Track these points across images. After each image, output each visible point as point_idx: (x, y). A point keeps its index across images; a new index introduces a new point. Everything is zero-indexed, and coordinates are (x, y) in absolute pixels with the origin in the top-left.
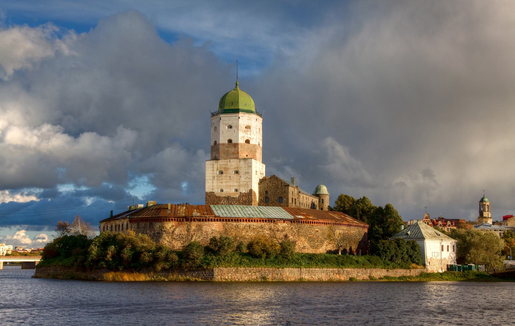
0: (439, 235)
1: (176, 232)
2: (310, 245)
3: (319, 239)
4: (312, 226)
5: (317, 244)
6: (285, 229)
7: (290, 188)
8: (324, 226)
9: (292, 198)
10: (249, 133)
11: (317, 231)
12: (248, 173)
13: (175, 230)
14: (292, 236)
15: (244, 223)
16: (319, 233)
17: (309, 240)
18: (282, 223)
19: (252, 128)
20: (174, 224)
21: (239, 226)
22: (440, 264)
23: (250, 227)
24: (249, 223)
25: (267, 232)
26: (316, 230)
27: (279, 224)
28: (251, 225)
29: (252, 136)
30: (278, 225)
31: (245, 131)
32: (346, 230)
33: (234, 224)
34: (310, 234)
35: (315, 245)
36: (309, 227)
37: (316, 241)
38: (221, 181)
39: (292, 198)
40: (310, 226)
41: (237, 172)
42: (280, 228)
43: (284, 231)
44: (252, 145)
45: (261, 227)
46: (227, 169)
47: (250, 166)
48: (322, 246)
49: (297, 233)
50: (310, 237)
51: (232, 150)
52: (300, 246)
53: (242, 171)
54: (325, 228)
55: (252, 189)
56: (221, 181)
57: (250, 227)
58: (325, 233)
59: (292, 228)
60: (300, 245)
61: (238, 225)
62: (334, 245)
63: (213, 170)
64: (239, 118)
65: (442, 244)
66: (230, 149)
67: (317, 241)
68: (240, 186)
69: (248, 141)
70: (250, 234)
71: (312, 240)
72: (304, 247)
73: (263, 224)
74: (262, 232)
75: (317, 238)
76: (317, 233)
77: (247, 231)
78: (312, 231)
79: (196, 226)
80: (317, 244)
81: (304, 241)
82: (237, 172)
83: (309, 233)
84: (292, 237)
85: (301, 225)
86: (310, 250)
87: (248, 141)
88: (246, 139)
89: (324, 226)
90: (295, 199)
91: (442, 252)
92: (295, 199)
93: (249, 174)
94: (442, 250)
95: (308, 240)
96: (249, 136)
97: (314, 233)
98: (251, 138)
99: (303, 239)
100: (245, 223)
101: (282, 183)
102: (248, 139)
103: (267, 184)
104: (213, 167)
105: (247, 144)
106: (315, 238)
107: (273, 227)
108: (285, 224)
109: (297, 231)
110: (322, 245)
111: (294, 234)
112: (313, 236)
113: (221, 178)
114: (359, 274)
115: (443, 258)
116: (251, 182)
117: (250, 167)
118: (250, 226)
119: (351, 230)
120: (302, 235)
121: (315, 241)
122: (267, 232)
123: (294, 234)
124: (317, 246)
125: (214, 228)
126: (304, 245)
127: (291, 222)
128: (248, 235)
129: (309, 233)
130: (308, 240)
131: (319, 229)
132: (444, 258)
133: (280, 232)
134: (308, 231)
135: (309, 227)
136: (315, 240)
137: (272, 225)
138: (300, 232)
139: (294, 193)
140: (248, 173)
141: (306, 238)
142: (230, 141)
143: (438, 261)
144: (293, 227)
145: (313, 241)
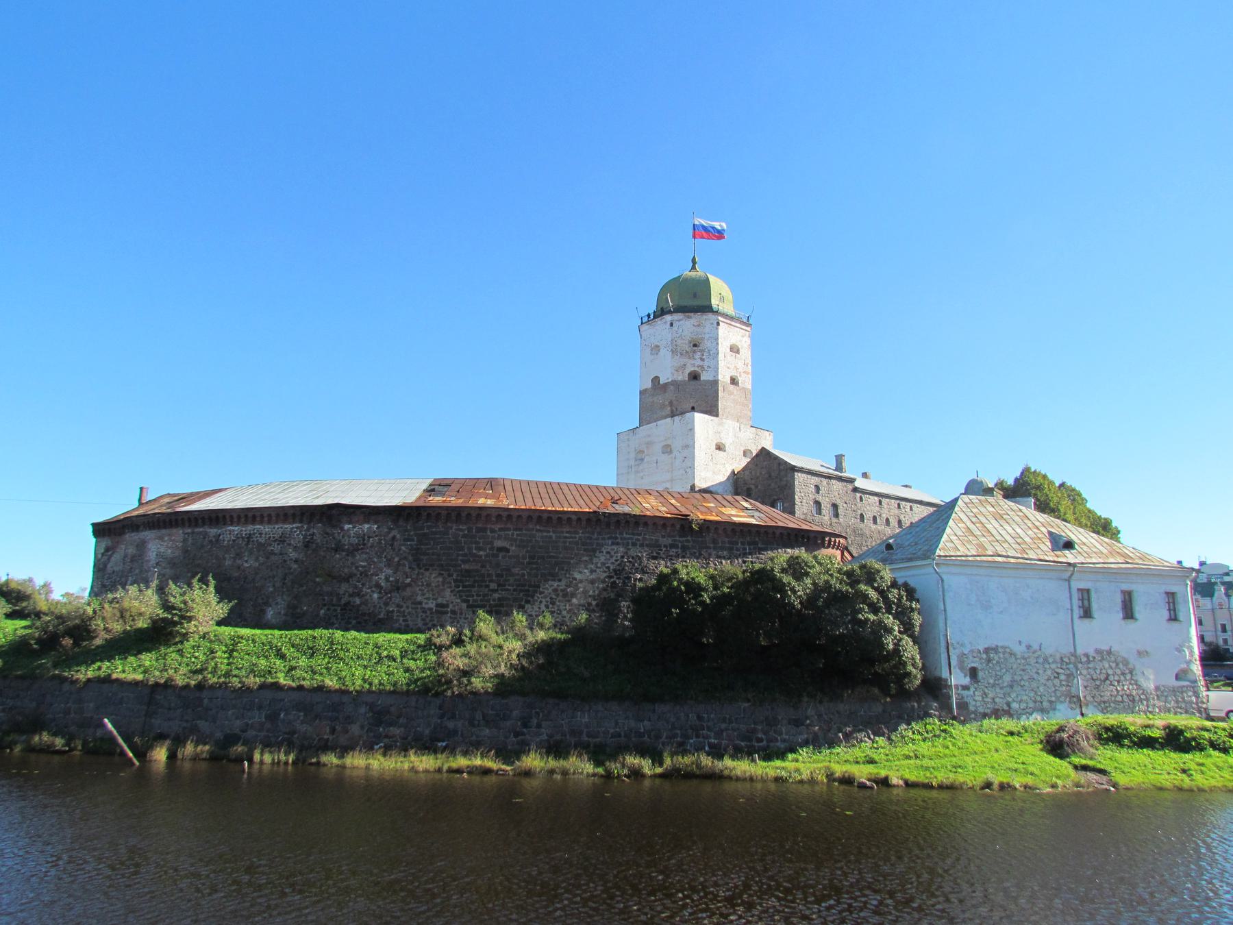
0: (1069, 545)
1: (109, 566)
2: (467, 601)
3: (512, 580)
4: (479, 530)
5: (496, 596)
6: (364, 544)
7: (798, 476)
8: (537, 530)
9: (818, 504)
10: (698, 355)
11: (500, 549)
12: (687, 447)
13: (109, 559)
14: (389, 565)
15: (237, 528)
16: (510, 557)
17: (461, 581)
18: (357, 522)
19: (707, 344)
20: (110, 543)
21: (221, 537)
22: (1062, 677)
23: (248, 542)
24: (250, 527)
25: (293, 555)
26: (498, 543)
27: (347, 527)
28: (254, 534)
29: (706, 364)
30: (342, 529)
31: (687, 352)
32: (676, 547)
33: (213, 531)
34: (464, 562)
35: (488, 601)
36: (464, 536)
37: (493, 586)
38: (642, 474)
39: (818, 504)
40: (470, 529)
41: (667, 449)
42: (346, 541)
43: (362, 549)
44: (708, 381)
45: (282, 540)
46: (649, 444)
47: (691, 430)
48: (526, 606)
49: (412, 555)
50: (467, 571)
51: (659, 399)
52: (420, 603)
53: (677, 444)
54: (542, 537)
55: (694, 485)
56: (642, 474)
57: (248, 542)
58: (543, 558)
59: (394, 538)
60: (419, 598)
61: (220, 535)
62: (594, 603)
63: (629, 453)
64: (672, 325)
65: (1077, 584)
66: (655, 399)
67: (499, 585)
68: (672, 480)
69: (695, 376)
70: (246, 565)
71: (475, 581)
72: (437, 605)
73: (288, 526)
74: (281, 554)
75: (498, 575)
76: (501, 555)
77: (237, 555)
78: (479, 549)
79: (137, 546)
80: (496, 596)
81: (439, 586)
82: (667, 449)
83: (462, 555)
84: (390, 572)
85: (429, 527)
86: (466, 619)
87: (695, 376)
88: (689, 369)
89: (537, 530)
90: (835, 506)
91: (1082, 626)
92: (835, 506)
93: (689, 447)
94: (1087, 614)
95: (455, 581)
96: (698, 362)
97: (487, 556)
98: (702, 367)
99: (433, 577)
100: (236, 529)
101: (779, 464)
102: (696, 369)
103: (751, 473)
104: (629, 446)
105: (693, 382)
106: (489, 575)
107: (318, 538)
108: (366, 526)
109: (410, 550)
110: (528, 602)
111: (396, 559)
112: (483, 566)
113: (641, 468)
114: (451, 725)
115: (1080, 651)
116: (692, 467)
117: (692, 430)
118: (249, 537)
119: (710, 548)
120: (432, 565)
121: (487, 586)
122: (293, 555)
123: (400, 560)
124: (502, 605)
125: (162, 550)
126: (440, 601)
127: (395, 521)
128: (239, 568)
129: (465, 555)
130: (455, 581)
131: (515, 540)
132: (1098, 652)
133: (344, 553)
134: (462, 549)
135: (464, 536)
136: (491, 581)
137: (317, 529)
138: (428, 554)
139: (823, 490)
140: (687, 447)
141: (450, 575)
142: (656, 380)
143: (1053, 666)
144: (398, 536)
145: (480, 586)
